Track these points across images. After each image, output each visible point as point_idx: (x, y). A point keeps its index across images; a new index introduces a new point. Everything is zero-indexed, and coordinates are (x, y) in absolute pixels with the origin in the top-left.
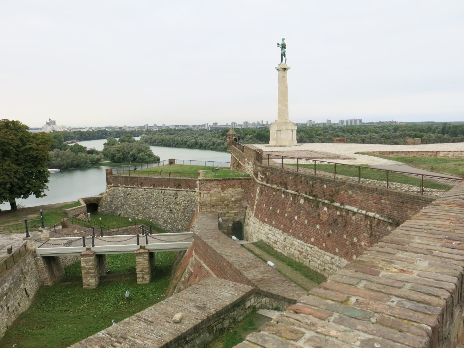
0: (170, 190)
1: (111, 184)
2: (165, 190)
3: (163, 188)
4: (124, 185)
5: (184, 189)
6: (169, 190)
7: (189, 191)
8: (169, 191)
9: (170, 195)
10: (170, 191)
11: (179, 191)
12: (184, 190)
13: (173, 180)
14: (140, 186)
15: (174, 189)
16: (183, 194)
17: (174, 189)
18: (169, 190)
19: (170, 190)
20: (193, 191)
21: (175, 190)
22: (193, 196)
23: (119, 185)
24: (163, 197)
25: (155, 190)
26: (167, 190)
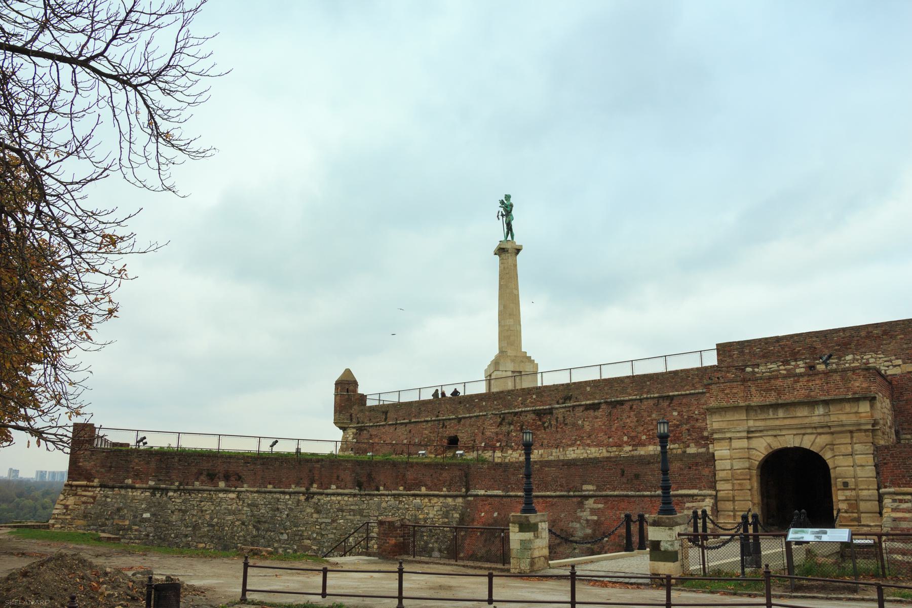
0: (338, 494)
1: (89, 480)
2: (321, 494)
3: (314, 488)
4: (152, 483)
5: (386, 489)
6: (333, 494)
7: (402, 495)
8: (333, 498)
9: (342, 511)
10: (339, 498)
11: (369, 495)
12: (387, 492)
13: (349, 465)
14: (222, 485)
15: (353, 491)
16: (384, 505)
17: (353, 491)
18: (333, 494)
19: (338, 494)
20: (415, 496)
21: (355, 495)
22: (419, 508)
23: (129, 481)
24: (315, 516)
25: (282, 497)
26: (327, 495)
